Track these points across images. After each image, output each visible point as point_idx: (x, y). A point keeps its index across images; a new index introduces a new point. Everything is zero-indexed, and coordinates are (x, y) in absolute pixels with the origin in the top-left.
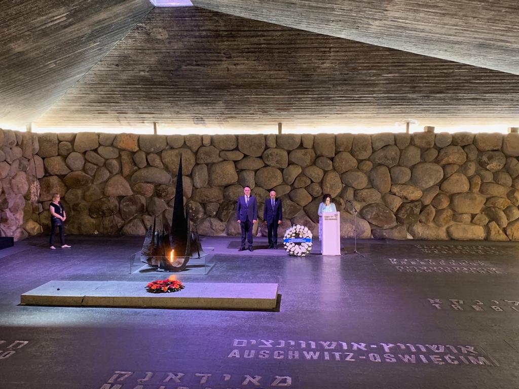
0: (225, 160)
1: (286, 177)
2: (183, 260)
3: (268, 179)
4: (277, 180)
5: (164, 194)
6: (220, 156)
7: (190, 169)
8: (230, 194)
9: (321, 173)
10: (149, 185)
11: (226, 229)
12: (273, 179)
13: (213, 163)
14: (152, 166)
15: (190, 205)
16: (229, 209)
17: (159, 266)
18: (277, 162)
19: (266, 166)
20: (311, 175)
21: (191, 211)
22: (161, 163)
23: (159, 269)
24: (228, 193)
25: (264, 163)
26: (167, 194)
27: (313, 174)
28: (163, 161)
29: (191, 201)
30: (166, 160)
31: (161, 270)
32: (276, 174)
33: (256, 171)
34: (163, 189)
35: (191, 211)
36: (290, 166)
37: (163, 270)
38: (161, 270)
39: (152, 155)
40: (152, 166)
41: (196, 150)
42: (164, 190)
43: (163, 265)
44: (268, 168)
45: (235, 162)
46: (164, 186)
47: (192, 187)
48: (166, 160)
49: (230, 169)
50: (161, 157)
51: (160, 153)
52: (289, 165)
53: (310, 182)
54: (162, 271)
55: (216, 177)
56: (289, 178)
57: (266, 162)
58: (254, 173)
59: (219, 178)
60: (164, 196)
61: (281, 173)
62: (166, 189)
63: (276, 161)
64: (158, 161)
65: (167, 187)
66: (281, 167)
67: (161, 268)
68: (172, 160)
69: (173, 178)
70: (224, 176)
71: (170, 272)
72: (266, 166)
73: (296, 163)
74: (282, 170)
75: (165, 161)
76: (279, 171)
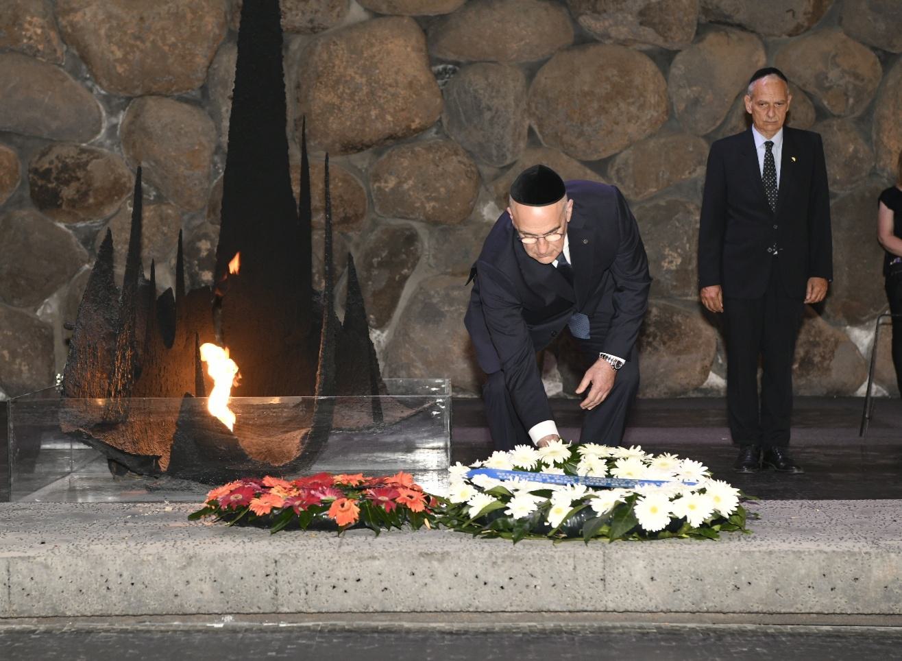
0: (376, 15)
1: (688, 92)
3: (595, 105)
4: (642, 107)
5: (68, 192)
7: (201, 61)
8: (406, 186)
9: (866, 63)
12: (622, 105)
16: (403, 264)
18: (645, 17)
19: (583, 40)
20: (821, 78)
24: (392, 182)
25: (575, 21)
26: (85, 195)
27: (833, 74)
28: (63, 22)
30: (77, 17)
32: (638, 80)
33: (532, 71)
34: (65, 168)
36: (711, 37)
42: (67, 173)
44: (592, 50)
45: (431, 28)
46: (67, 152)
48: (77, 17)
49: (400, 55)
52: (701, 31)
53: (812, 115)
55: (331, 98)
56: (709, 97)
57: (588, 22)
58: (521, 76)
59: (348, 105)
60: (73, 203)
61: (660, 75)
62: (83, 166)
63: (641, 13)
65: (84, 157)
66: (660, 42)
68: (110, 17)
69: (112, 112)
70: (372, 93)
72: (583, 40)
73: (740, 17)
74: (664, 58)
75: (72, 25)
76: (650, 67)
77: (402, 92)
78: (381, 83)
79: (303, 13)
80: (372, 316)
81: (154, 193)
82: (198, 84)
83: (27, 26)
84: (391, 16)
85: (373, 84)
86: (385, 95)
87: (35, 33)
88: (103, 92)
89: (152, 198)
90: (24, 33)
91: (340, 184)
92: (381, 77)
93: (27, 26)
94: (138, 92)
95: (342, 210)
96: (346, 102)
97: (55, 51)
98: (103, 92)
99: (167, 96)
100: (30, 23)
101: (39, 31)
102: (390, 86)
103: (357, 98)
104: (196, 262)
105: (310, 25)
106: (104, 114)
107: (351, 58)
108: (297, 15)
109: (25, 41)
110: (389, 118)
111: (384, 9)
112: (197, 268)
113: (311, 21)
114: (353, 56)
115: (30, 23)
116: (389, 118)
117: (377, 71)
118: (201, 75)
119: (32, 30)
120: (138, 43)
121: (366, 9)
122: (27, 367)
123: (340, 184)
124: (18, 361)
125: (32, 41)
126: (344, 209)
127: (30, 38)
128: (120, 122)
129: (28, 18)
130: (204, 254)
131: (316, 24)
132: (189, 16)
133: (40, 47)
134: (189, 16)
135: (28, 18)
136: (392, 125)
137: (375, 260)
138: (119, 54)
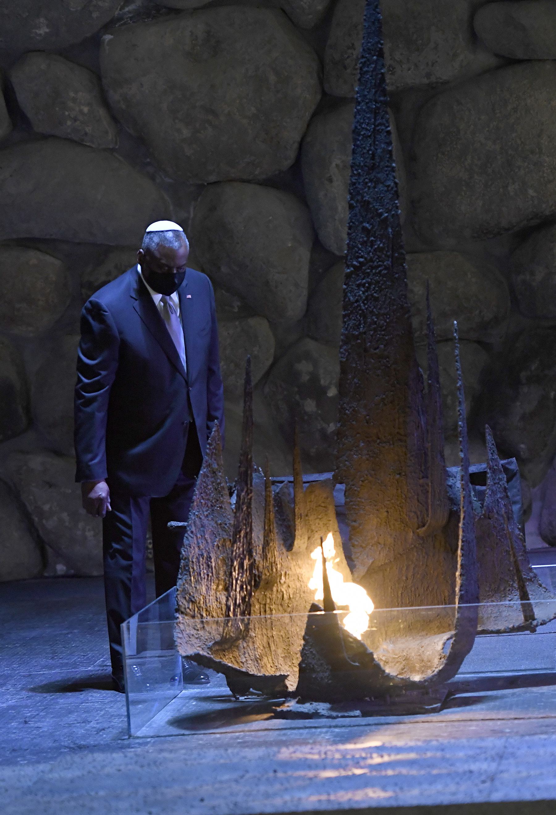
0: (508, 62)
2: (433, 648)
6: (474, 38)
7: (292, 134)
10: (33, 257)
11: (536, 507)
13: (433, 91)
14: (45, 137)
15: (304, 368)
17: (292, 684)
21: (310, 406)
22: (101, 112)
23: (291, 705)
28: (114, 96)
29: (311, 345)
31: (307, 707)
35: (310, 406)
37: (322, 707)
38: (307, 707)
39: (38, 64)
40: (45, 137)
41: (320, 8)
43: (323, 675)
47: (304, 254)
50: (97, 76)
51: (84, 52)
54: (315, 715)
64: (80, 103)
67: (302, 694)
71: (365, 714)
77: (547, 159)
78: (520, 149)
79: (416, 66)
80: (522, 446)
81: (239, 304)
82: (287, 163)
83: (70, 104)
84: (529, 61)
85: (510, 152)
86: (526, 164)
87: (81, 112)
88: (168, 180)
89: (236, 310)
90: (67, 113)
91: (474, 280)
92: (519, 142)
93: (70, 104)
94: (212, 178)
95: (477, 312)
96: (476, 177)
97: (107, 132)
98: (168, 180)
99: (249, 181)
100: (74, 100)
101: (86, 110)
102: (532, 152)
103: (490, 171)
104: (296, 389)
105: (425, 81)
106: (171, 208)
107: (479, 119)
108: (409, 70)
109: (69, 123)
110: (531, 192)
111: (520, 54)
112: (297, 397)
113: (428, 75)
114: (483, 117)
115: (74, 100)
116: (531, 192)
117: (514, 135)
118: (292, 154)
119: (77, 109)
120: (210, 117)
121: (497, 55)
122: (92, 533)
123: (474, 280)
124: (81, 525)
125: (78, 123)
126: (480, 312)
127: (75, 120)
128: (192, 215)
129: (72, 94)
130: (305, 378)
131: (433, 79)
132: (272, 78)
133: (88, 129)
134: (272, 78)
135: (72, 94)
136: (536, 202)
137: (523, 375)
138: (186, 133)
